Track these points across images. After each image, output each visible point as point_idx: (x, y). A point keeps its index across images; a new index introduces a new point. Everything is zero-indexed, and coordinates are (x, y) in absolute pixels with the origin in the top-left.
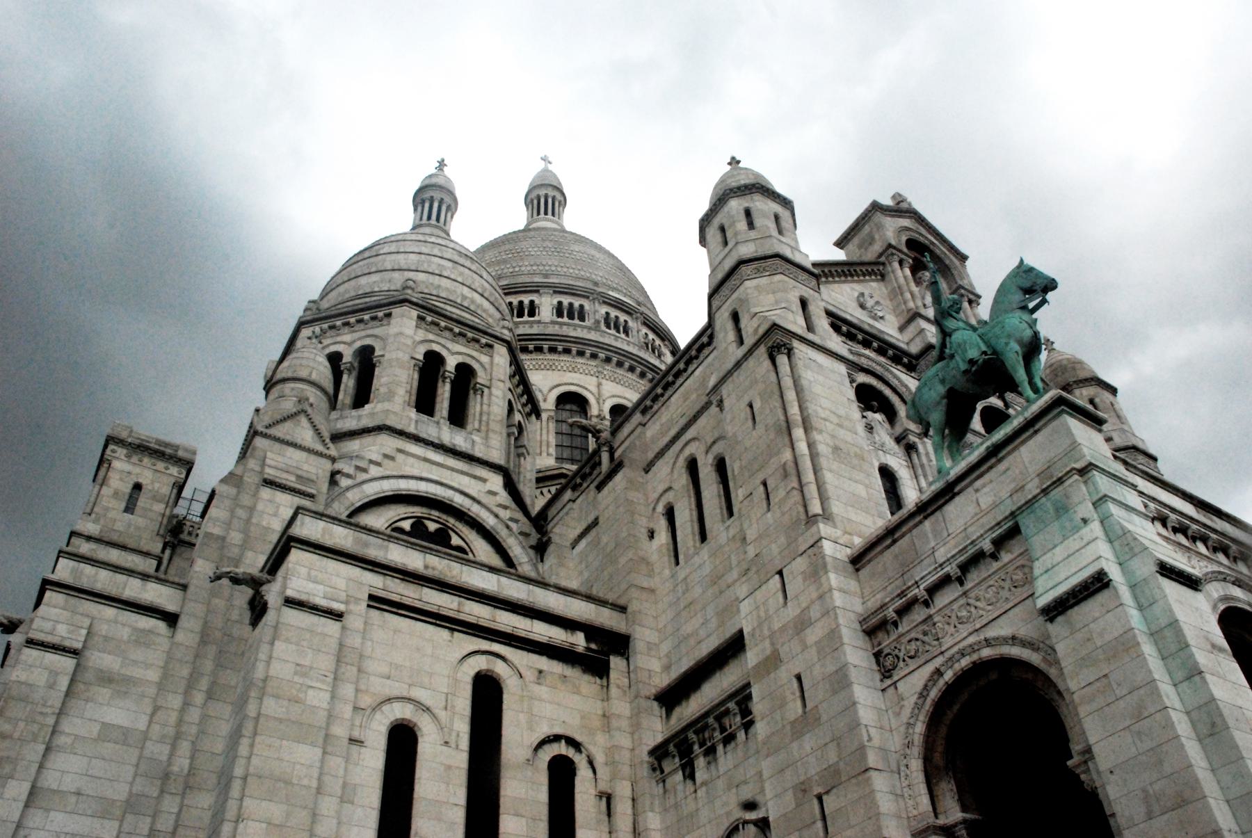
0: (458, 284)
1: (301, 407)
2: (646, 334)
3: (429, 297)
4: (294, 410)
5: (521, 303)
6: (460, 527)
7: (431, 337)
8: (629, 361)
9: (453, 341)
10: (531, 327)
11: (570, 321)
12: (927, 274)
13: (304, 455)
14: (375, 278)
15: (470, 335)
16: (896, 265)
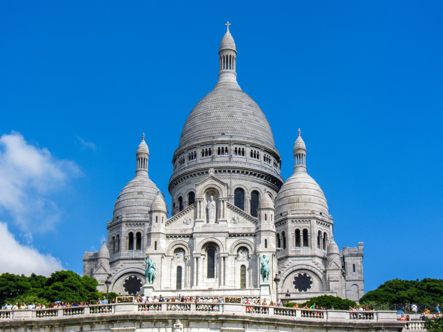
0: (136, 206)
1: (101, 265)
2: (236, 148)
3: (130, 215)
4: (100, 266)
5: (192, 153)
6: (138, 275)
7: (130, 228)
8: (222, 169)
9: (135, 227)
10: (192, 167)
11: (206, 157)
12: (212, 197)
13: (103, 275)
14: (119, 210)
15: (138, 224)
16: (198, 203)
